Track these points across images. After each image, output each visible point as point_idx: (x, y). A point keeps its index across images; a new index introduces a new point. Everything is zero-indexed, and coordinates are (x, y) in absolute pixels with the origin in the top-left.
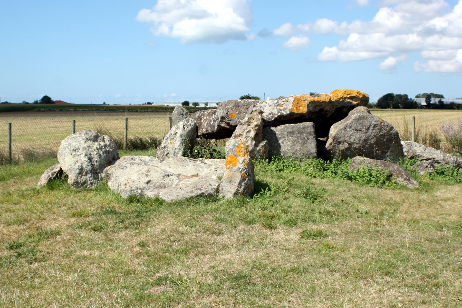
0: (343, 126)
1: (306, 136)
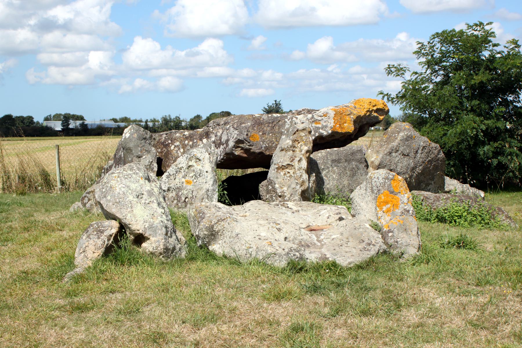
0: (388, 150)
1: (356, 166)
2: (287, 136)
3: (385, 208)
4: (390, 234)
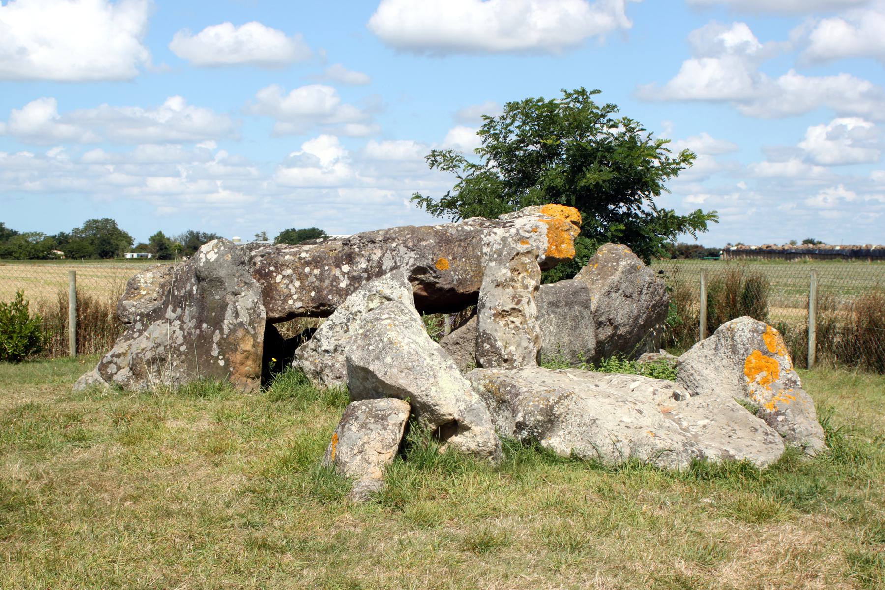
0: (606, 288)
1: (580, 312)
2: (500, 263)
3: (758, 378)
4: (780, 418)
